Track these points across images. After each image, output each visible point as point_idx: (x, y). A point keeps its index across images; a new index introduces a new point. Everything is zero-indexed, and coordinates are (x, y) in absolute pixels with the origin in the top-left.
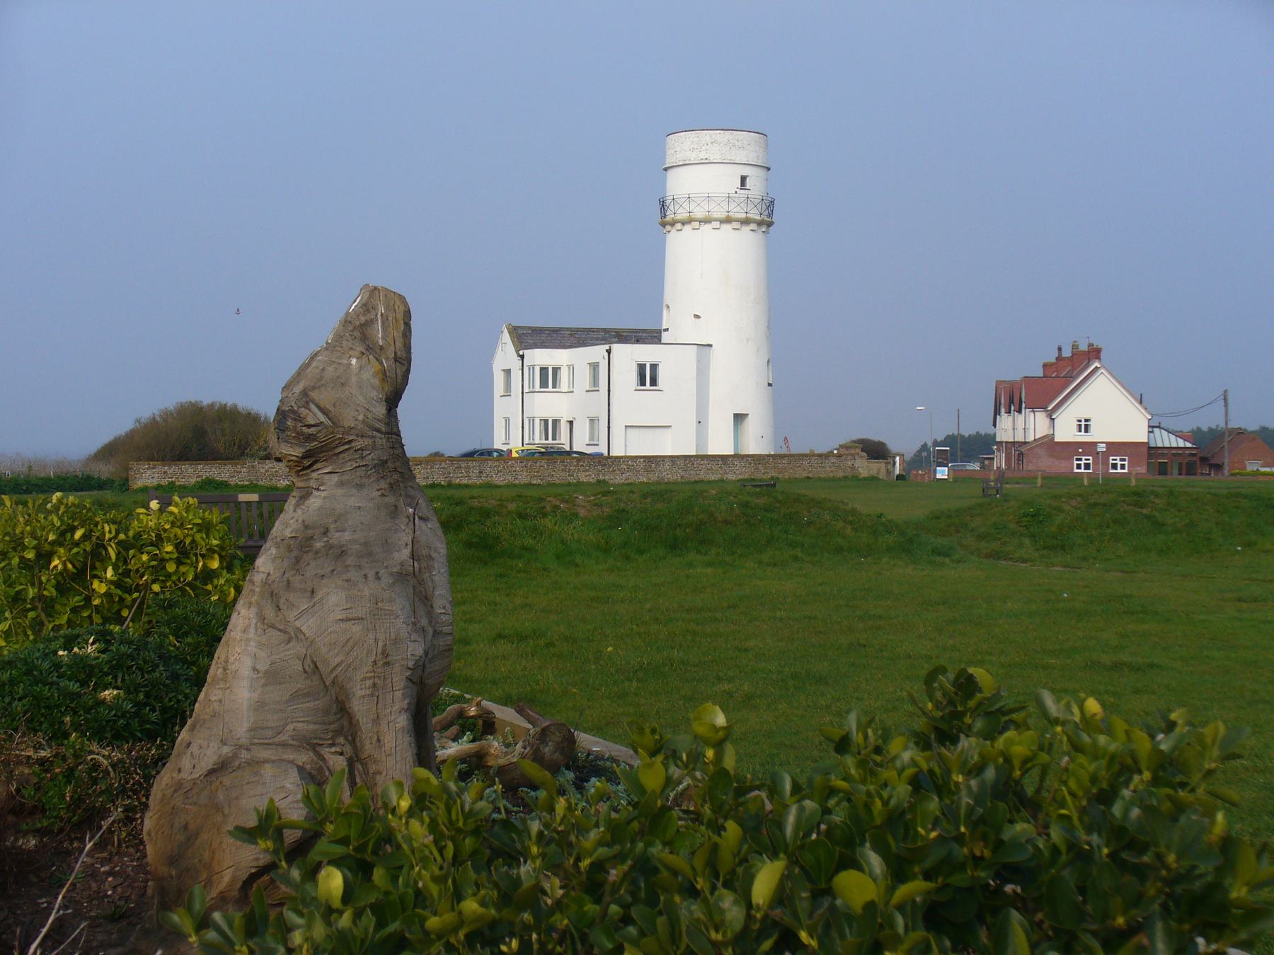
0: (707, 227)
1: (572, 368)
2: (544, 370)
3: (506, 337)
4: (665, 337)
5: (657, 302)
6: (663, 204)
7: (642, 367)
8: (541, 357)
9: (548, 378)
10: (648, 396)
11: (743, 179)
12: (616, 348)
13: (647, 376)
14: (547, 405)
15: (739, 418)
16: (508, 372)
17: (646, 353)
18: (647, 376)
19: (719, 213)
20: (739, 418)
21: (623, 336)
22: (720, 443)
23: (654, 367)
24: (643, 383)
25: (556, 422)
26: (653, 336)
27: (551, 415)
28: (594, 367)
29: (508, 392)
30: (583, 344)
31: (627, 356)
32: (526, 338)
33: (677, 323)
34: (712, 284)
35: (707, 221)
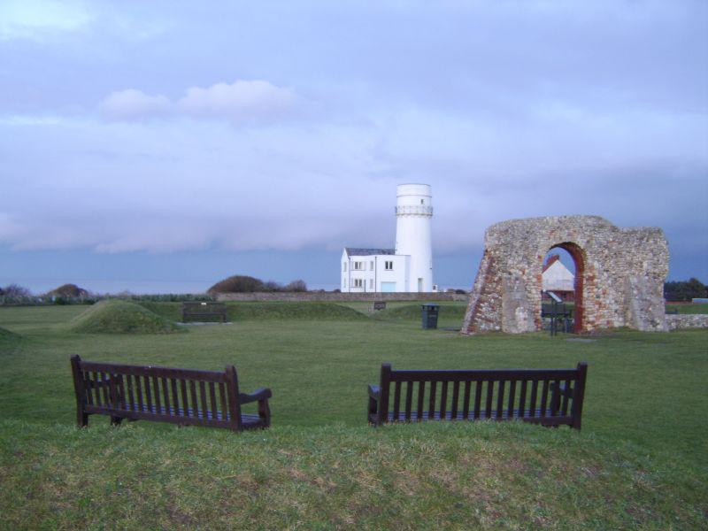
0: (409, 217)
1: (365, 263)
2: (356, 264)
3: (345, 252)
4: (397, 253)
5: (393, 241)
6: (396, 209)
7: (387, 263)
8: (356, 258)
9: (357, 265)
10: (389, 272)
11: (422, 201)
12: (379, 256)
13: (389, 266)
14: (357, 275)
15: (420, 280)
16: (345, 264)
17: (388, 258)
18: (389, 266)
19: (414, 212)
20: (420, 280)
21: (384, 252)
22: (414, 289)
23: (391, 264)
24: (387, 267)
25: (361, 281)
26: (391, 252)
27: (358, 277)
28: (372, 263)
29: (345, 271)
30: (370, 254)
31: (382, 259)
32: (351, 252)
33: (400, 249)
34: (412, 239)
35: (409, 214)
